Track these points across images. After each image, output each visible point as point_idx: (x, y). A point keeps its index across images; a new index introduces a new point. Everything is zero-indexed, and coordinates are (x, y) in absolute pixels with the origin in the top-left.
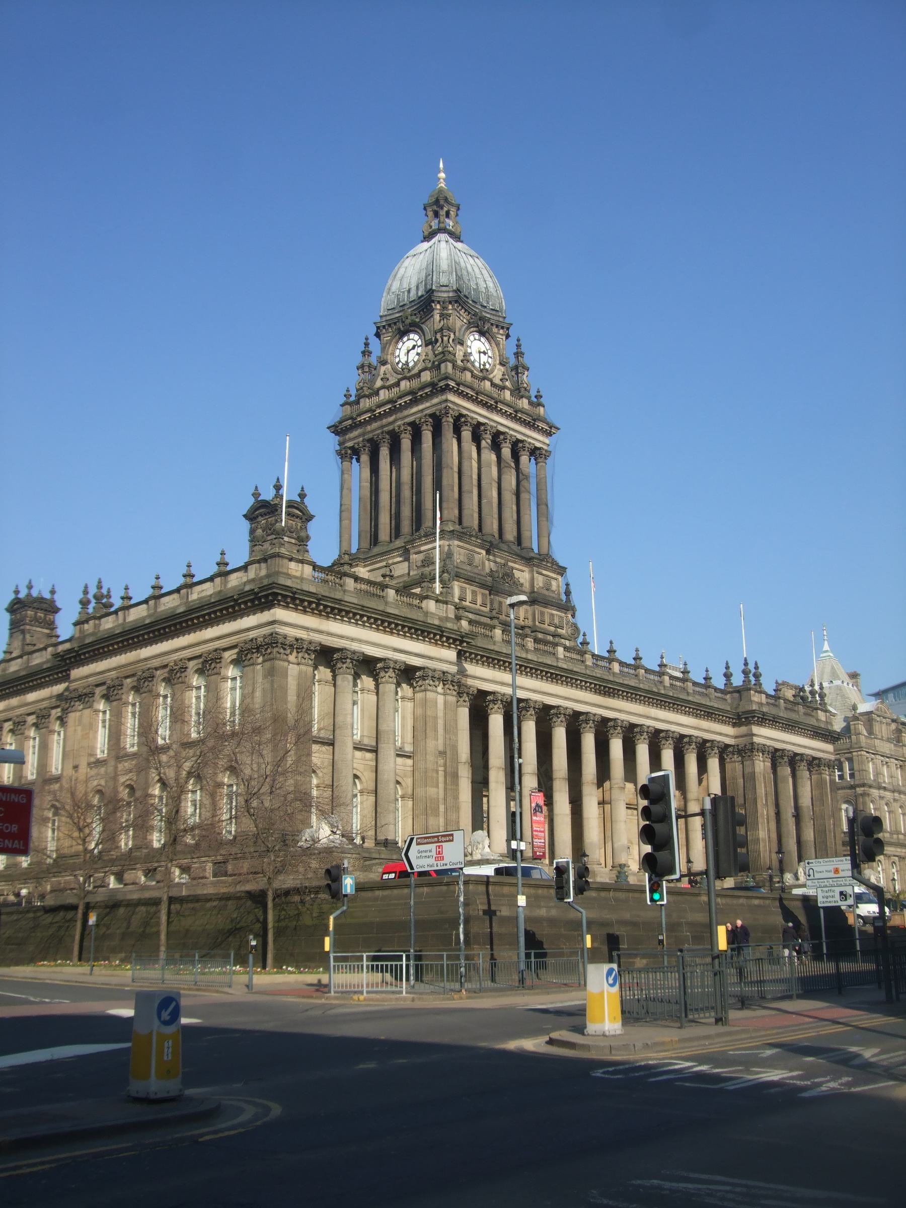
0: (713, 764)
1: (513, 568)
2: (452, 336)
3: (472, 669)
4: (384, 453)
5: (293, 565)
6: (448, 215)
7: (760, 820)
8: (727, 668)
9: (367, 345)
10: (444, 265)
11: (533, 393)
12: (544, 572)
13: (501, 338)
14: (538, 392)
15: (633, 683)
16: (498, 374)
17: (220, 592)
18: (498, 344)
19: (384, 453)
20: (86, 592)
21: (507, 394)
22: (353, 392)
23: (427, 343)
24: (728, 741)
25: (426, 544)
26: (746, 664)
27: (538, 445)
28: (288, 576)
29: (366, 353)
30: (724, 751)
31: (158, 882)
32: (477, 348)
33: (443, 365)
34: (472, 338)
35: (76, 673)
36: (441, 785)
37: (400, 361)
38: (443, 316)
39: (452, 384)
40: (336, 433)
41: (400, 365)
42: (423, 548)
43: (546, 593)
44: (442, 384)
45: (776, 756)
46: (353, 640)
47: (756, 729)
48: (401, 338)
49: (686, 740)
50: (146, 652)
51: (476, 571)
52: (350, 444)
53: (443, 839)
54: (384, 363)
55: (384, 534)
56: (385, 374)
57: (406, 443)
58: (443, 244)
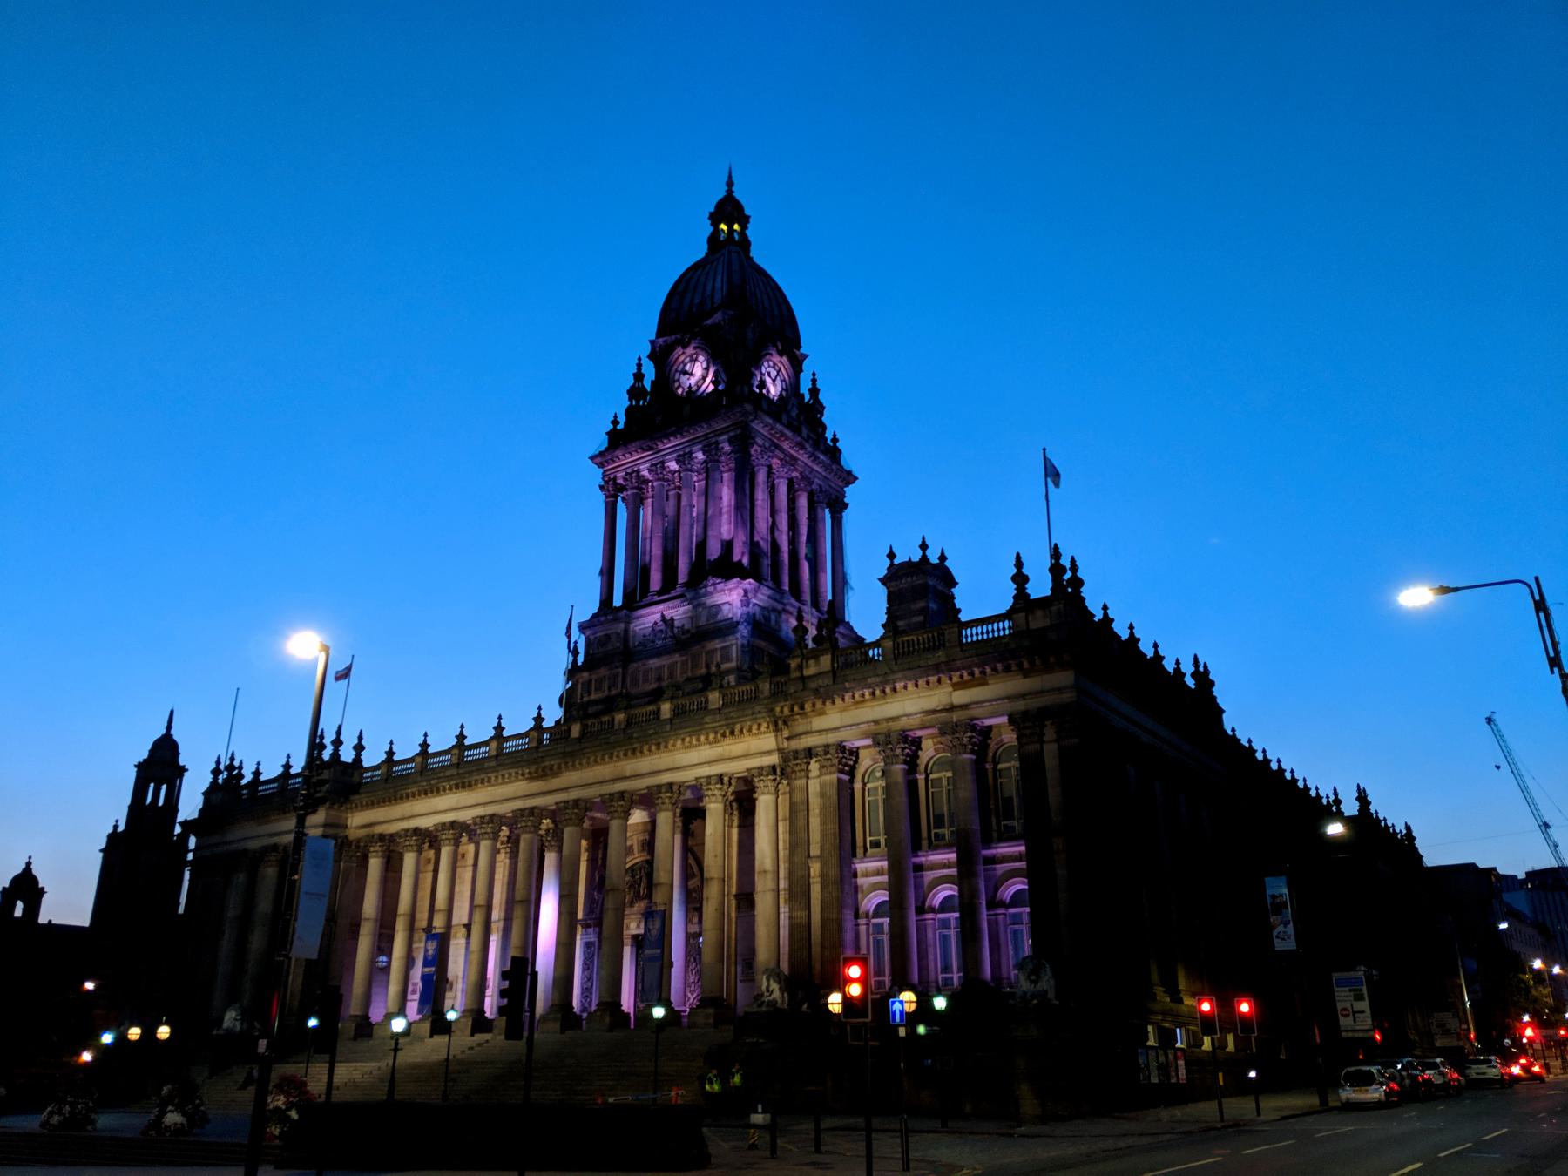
9: (639, 366)
11: (829, 435)
22: (622, 419)
29: (639, 376)
40: (601, 465)
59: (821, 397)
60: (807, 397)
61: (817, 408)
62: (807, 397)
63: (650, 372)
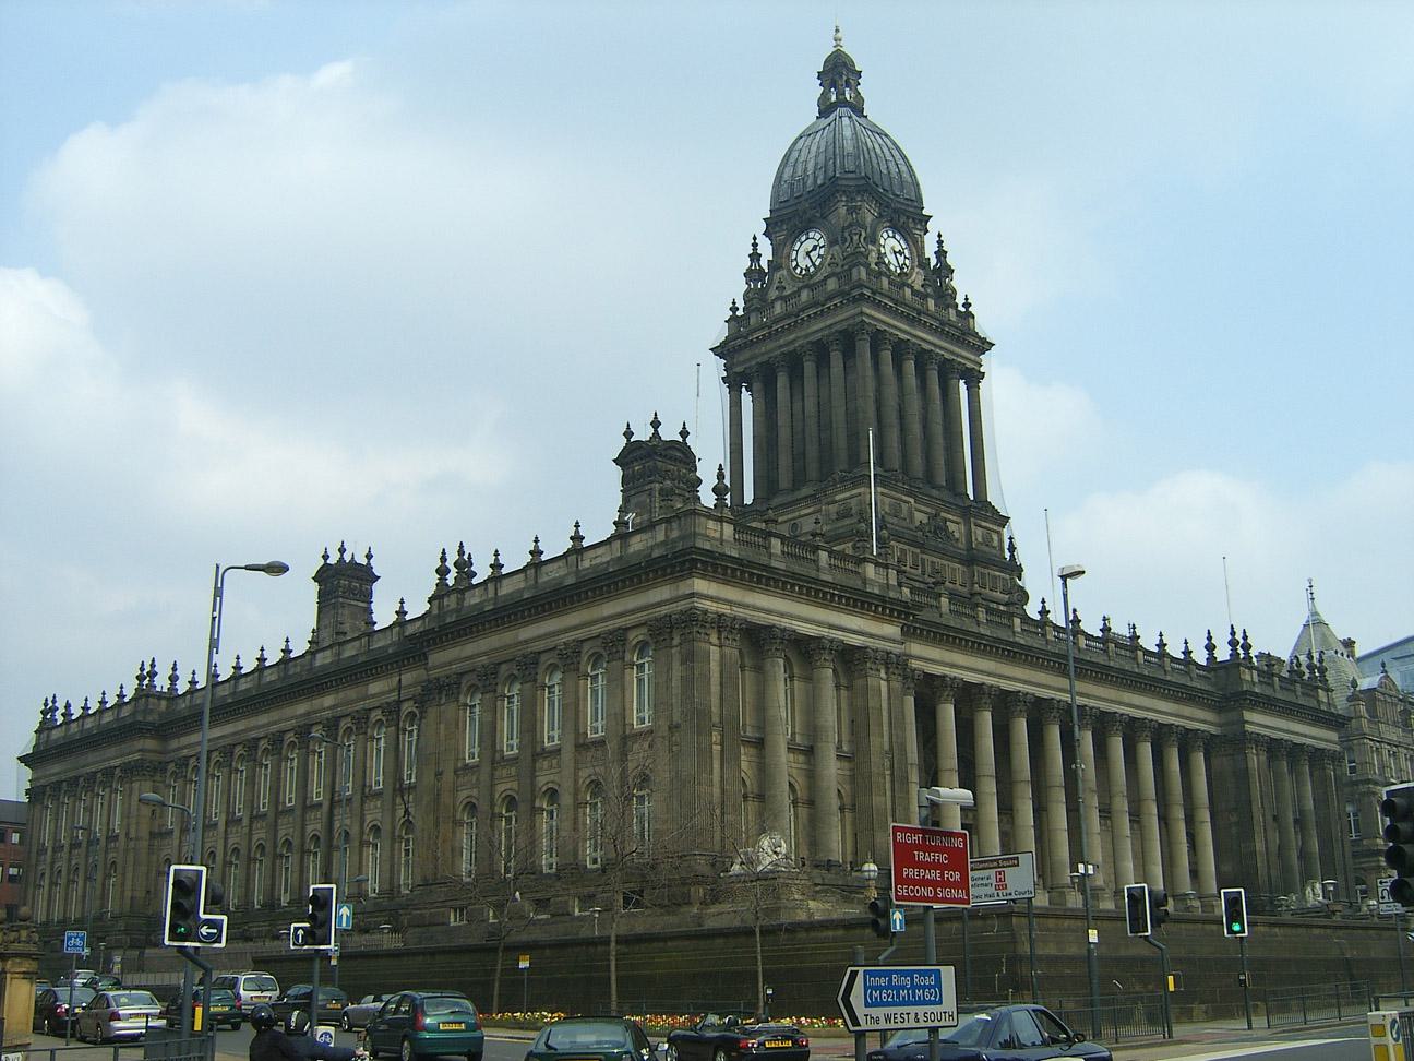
0: (1199, 759)
1: (946, 520)
2: (864, 234)
3: (916, 648)
4: (782, 381)
7: (1256, 828)
8: (1209, 638)
9: (755, 245)
10: (849, 147)
11: (960, 300)
12: (984, 524)
14: (966, 299)
15: (1101, 660)
16: (917, 279)
17: (620, 558)
19: (782, 381)
20: (443, 559)
21: (931, 303)
22: (741, 304)
23: (832, 243)
24: (1213, 730)
25: (842, 492)
26: (1233, 633)
28: (708, 538)
29: (755, 257)
30: (1210, 744)
31: (553, 915)
33: (854, 271)
34: (885, 235)
35: (436, 658)
36: (889, 793)
37: (797, 265)
38: (851, 210)
41: (798, 270)
42: (838, 498)
43: (986, 549)
44: (855, 293)
45: (1273, 747)
46: (782, 615)
47: (1248, 715)
49: (1165, 730)
50: (526, 633)
51: (904, 524)
52: (739, 369)
53: (1005, 863)
55: (784, 481)
56: (780, 282)
57: (809, 368)
58: (846, 121)
59: (950, 260)
60: (933, 261)
61: (944, 271)
62: (933, 261)
63: (766, 250)
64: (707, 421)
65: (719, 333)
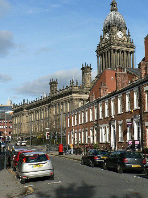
4: (103, 56)
5: (75, 87)
6: (115, 6)
9: (101, 34)
11: (131, 40)
13: (125, 31)
18: (124, 32)
22: (99, 44)
27: (132, 51)
28: (74, 89)
29: (101, 36)
32: (119, 34)
39: (112, 44)
48: (106, 33)
54: (104, 38)
57: (106, 54)
59: (130, 34)
64: (94, 62)
65: (96, 48)
